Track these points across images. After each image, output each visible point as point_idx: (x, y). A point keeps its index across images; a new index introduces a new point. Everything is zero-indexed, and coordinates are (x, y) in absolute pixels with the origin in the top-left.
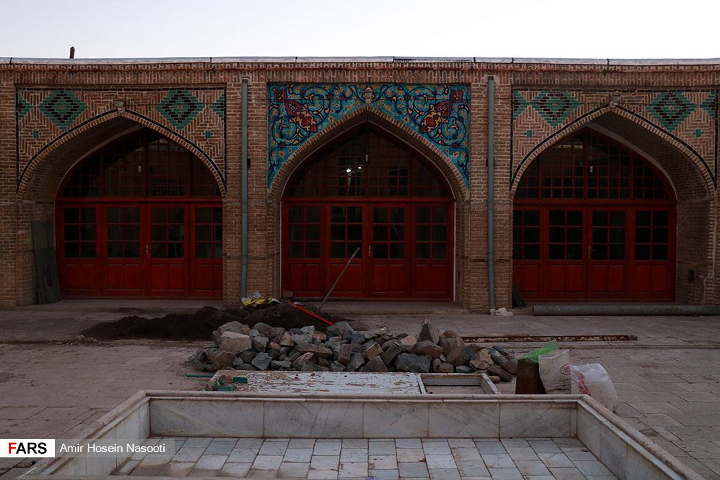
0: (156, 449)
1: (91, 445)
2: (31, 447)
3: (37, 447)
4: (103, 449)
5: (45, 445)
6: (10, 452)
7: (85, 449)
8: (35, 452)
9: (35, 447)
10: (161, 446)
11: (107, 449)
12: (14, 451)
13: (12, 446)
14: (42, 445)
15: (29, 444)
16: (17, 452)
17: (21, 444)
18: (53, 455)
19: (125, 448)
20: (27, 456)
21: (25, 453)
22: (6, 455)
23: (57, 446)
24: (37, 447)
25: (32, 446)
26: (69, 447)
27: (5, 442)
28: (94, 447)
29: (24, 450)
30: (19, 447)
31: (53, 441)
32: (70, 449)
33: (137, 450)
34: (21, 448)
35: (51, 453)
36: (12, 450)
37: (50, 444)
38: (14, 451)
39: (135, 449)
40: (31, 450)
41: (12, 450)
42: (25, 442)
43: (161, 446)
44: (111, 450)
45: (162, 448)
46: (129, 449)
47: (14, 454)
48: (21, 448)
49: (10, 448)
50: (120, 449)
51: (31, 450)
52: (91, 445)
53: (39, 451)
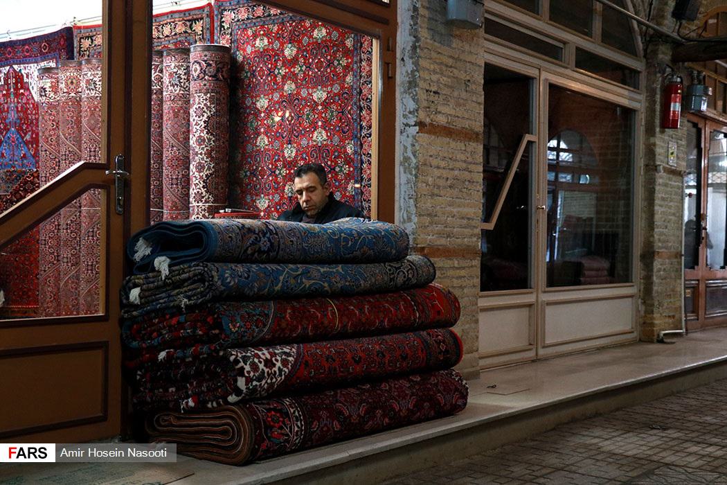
0: (158, 454)
1: (92, 450)
3: (38, 451)
4: (104, 454)
5: (45, 449)
6: (10, 457)
7: (86, 454)
8: (36, 457)
9: (36, 452)
10: (162, 451)
11: (108, 453)
12: (14, 456)
13: (12, 450)
14: (42, 450)
15: (29, 449)
16: (18, 457)
17: (21, 449)
18: (53, 460)
19: (126, 453)
20: (27, 460)
21: (25, 457)
22: (6, 459)
23: (58, 451)
24: (38, 451)
25: (32, 451)
26: (69, 452)
27: (5, 447)
29: (24, 455)
30: (20, 452)
31: (53, 445)
32: (71, 453)
33: (139, 455)
34: (21, 453)
35: (51, 458)
36: (12, 455)
37: (51, 448)
38: (14, 456)
39: (136, 453)
40: (31, 455)
41: (12, 455)
42: (25, 446)
43: (162, 451)
44: (112, 455)
47: (14, 459)
48: (21, 453)
49: (10, 453)
50: (121, 453)
51: (31, 455)
52: (92, 450)
53: (39, 456)
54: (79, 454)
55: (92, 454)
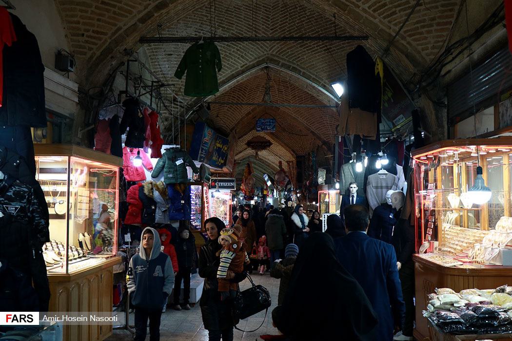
0: (111, 319)
3: (27, 317)
5: (32, 316)
6: (7, 321)
8: (25, 321)
9: (25, 318)
10: (114, 317)
11: (76, 319)
12: (10, 321)
13: (9, 317)
14: (30, 316)
15: (21, 315)
16: (12, 321)
17: (15, 316)
18: (38, 324)
20: (19, 324)
21: (18, 322)
22: (3, 322)
23: (41, 318)
24: (27, 317)
25: (23, 317)
26: (49, 318)
27: (4, 314)
29: (17, 320)
30: (14, 317)
31: (38, 313)
32: (50, 319)
33: (98, 320)
34: (15, 318)
35: (36, 322)
37: (36, 315)
38: (10, 321)
39: (96, 319)
40: (22, 320)
42: (18, 314)
43: (114, 317)
44: (79, 320)
45: (115, 320)
47: (10, 323)
48: (15, 318)
49: (7, 318)
50: (85, 319)
51: (22, 320)
53: (28, 321)
55: (65, 319)
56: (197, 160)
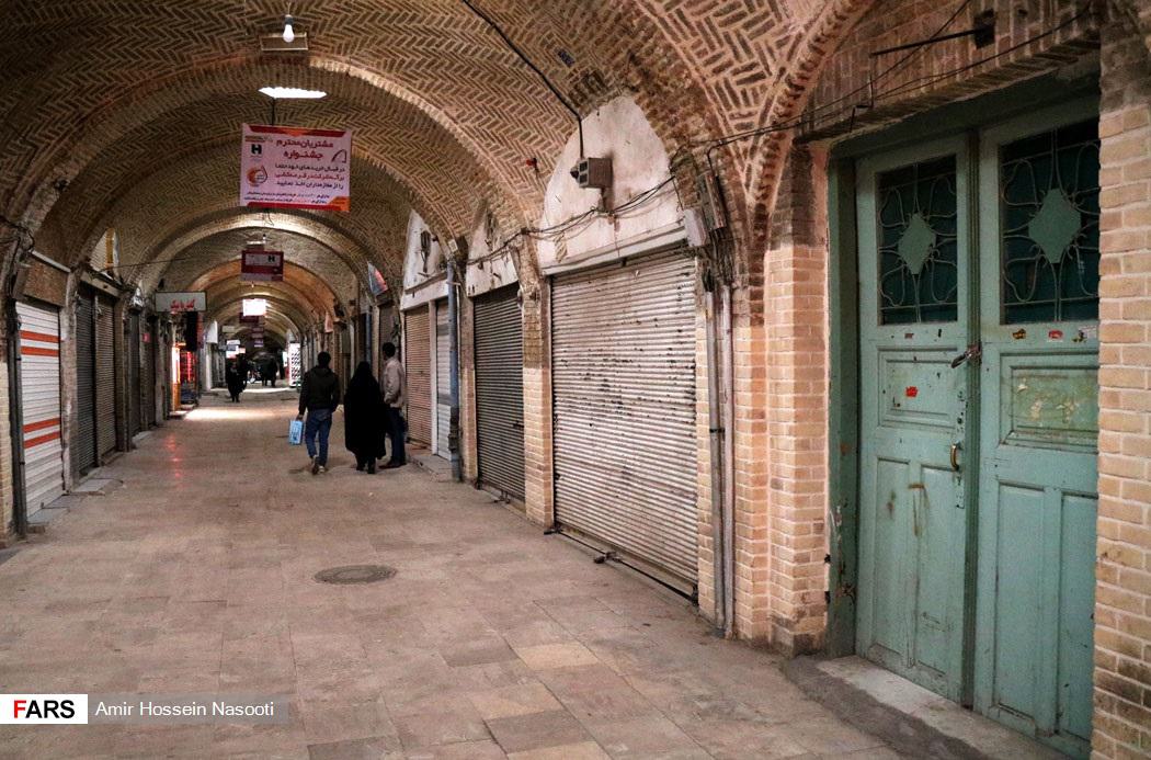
1: (146, 705)
2: (50, 708)
3: (60, 707)
4: (165, 710)
5: (72, 704)
6: (16, 716)
8: (57, 716)
9: (56, 707)
13: (20, 705)
14: (67, 705)
15: (46, 702)
16: (28, 716)
17: (34, 703)
18: (84, 721)
20: (43, 721)
21: (40, 716)
22: (9, 719)
23: (92, 706)
24: (60, 707)
25: (51, 706)
27: (9, 699)
28: (150, 708)
29: (38, 712)
30: (31, 707)
31: (85, 697)
32: (112, 710)
34: (34, 709)
35: (81, 717)
36: (19, 712)
41: (19, 712)
42: (40, 699)
43: (267, 707)
45: (269, 709)
46: (220, 706)
47: (22, 719)
48: (33, 709)
49: (17, 709)
52: (146, 705)
53: (62, 714)
54: (126, 711)
55: (146, 711)
56: (432, 301)
